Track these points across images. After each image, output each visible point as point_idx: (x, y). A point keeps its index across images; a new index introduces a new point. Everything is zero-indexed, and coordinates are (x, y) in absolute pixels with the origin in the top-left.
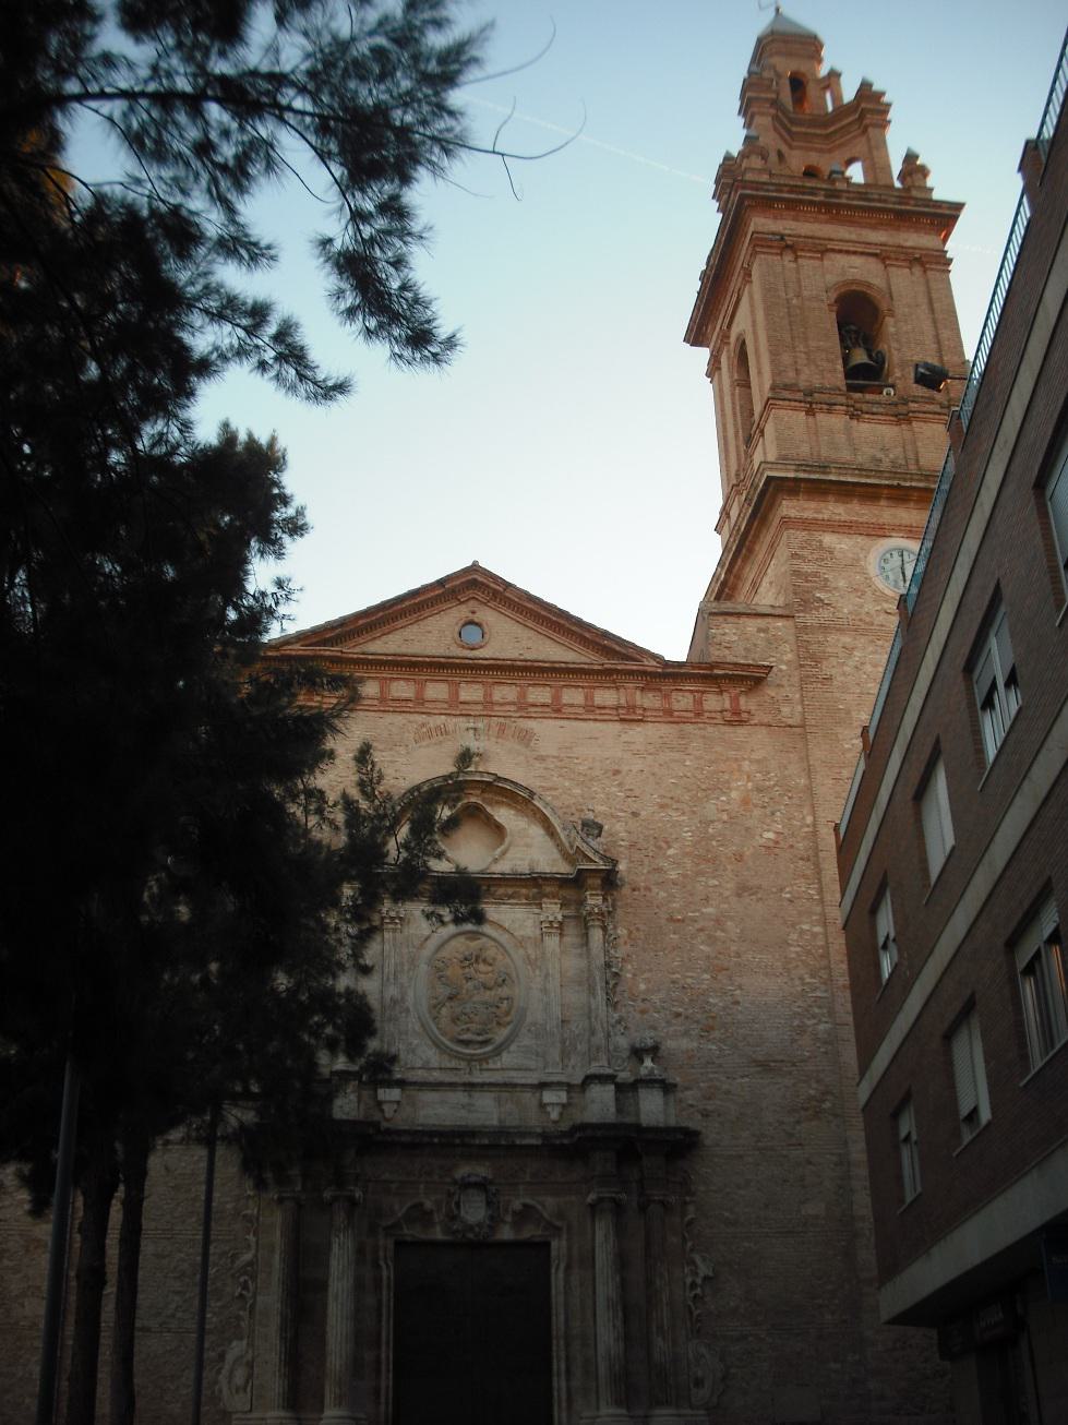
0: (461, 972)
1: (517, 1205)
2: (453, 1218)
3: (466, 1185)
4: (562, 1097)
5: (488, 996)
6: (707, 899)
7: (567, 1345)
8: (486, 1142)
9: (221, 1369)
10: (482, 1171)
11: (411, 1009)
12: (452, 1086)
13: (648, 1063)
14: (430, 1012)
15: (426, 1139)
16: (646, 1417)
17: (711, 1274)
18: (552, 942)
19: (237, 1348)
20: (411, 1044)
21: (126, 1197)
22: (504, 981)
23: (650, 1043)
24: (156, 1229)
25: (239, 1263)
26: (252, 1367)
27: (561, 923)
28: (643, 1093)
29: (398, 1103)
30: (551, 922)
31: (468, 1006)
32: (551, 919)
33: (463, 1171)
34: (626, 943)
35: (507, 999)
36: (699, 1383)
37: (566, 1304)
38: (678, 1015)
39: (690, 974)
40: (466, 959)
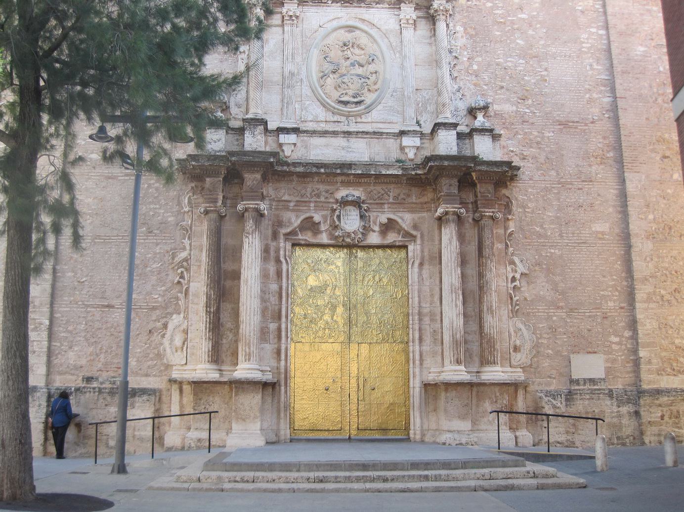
0: (341, 54)
1: (383, 219)
2: (336, 227)
3: (344, 203)
4: (417, 141)
5: (360, 71)
6: (521, 9)
7: (420, 320)
8: (360, 172)
9: (164, 334)
10: (356, 193)
12: (335, 133)
13: (480, 117)
14: (319, 82)
15: (314, 170)
16: (478, 372)
17: (527, 272)
18: (408, 33)
19: (176, 320)
20: (305, 104)
21: (41, 128)
22: (373, 60)
23: (482, 104)
24: (118, 236)
25: (177, 260)
26: (187, 334)
27: (415, 21)
28: (477, 138)
29: (295, 144)
30: (407, 20)
32: (408, 17)
33: (342, 193)
34: (462, 37)
35: (376, 73)
36: (516, 349)
37: (419, 291)
38: (502, 87)
39: (509, 59)
40: (345, 45)
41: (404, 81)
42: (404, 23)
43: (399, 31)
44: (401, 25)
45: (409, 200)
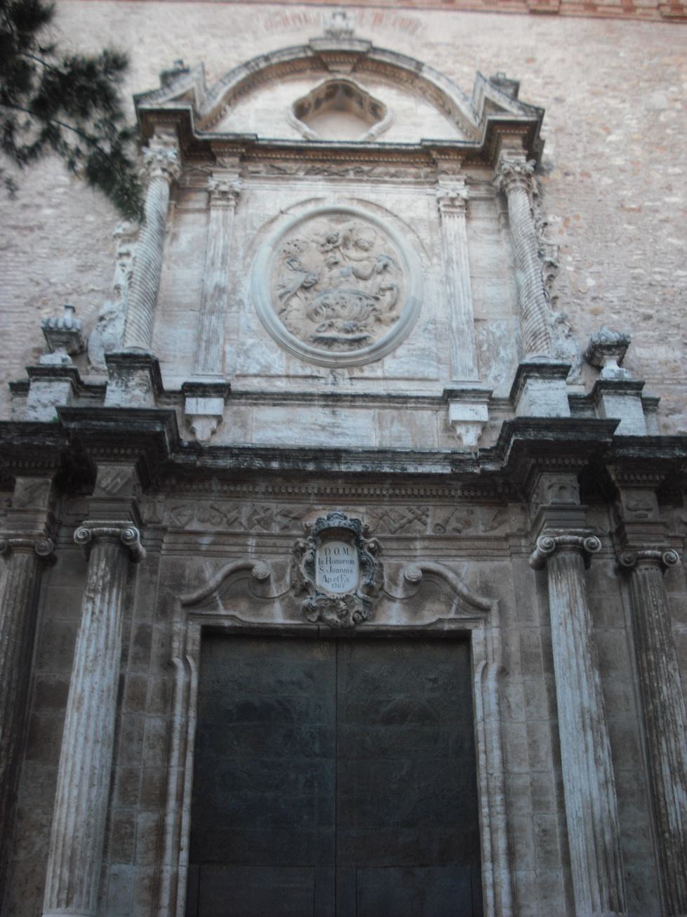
0: (322, 257)
1: (412, 570)
2: (305, 589)
3: (326, 535)
7: (508, 805)
8: (358, 468)
11: (246, 301)
12: (305, 399)
14: (274, 304)
15: (258, 463)
18: (455, 224)
23: (614, 337)
29: (219, 419)
30: (452, 199)
31: (331, 296)
32: (453, 195)
34: (561, 232)
35: (391, 289)
37: (502, 735)
39: (657, 269)
40: (329, 241)
41: (449, 302)
42: (445, 206)
43: (437, 221)
44: (439, 210)
45: (471, 532)
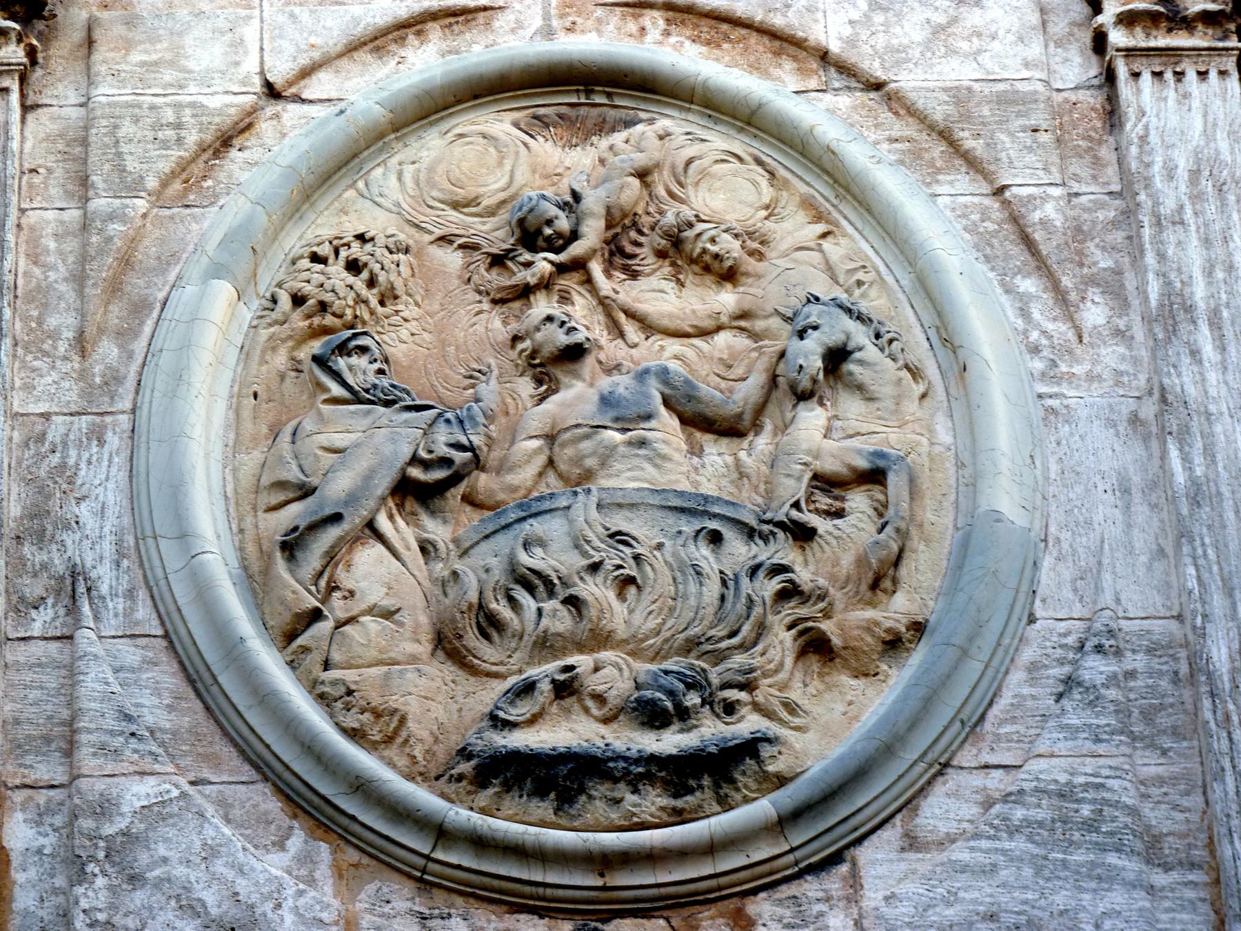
0: (496, 325)
11: (105, 576)
22: (837, 357)
31: (551, 527)
41: (1184, 534)
42: (1128, 20)
43: (1092, 99)
44: (1099, 42)
